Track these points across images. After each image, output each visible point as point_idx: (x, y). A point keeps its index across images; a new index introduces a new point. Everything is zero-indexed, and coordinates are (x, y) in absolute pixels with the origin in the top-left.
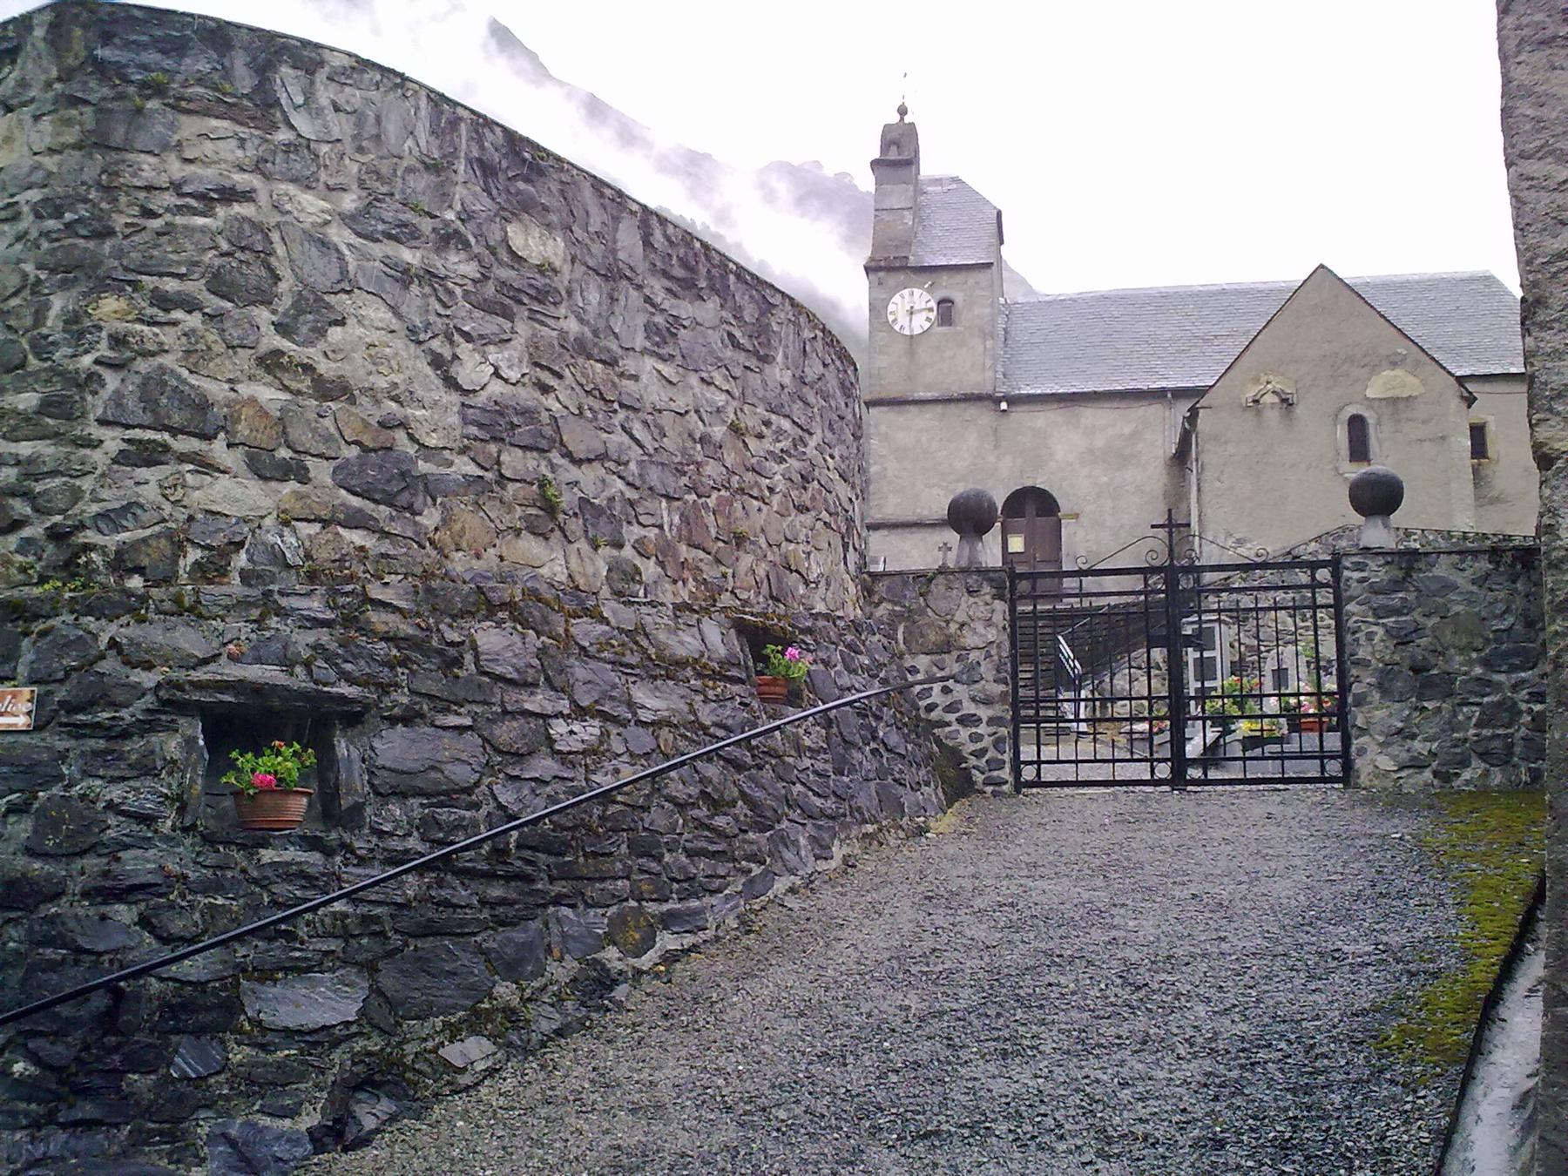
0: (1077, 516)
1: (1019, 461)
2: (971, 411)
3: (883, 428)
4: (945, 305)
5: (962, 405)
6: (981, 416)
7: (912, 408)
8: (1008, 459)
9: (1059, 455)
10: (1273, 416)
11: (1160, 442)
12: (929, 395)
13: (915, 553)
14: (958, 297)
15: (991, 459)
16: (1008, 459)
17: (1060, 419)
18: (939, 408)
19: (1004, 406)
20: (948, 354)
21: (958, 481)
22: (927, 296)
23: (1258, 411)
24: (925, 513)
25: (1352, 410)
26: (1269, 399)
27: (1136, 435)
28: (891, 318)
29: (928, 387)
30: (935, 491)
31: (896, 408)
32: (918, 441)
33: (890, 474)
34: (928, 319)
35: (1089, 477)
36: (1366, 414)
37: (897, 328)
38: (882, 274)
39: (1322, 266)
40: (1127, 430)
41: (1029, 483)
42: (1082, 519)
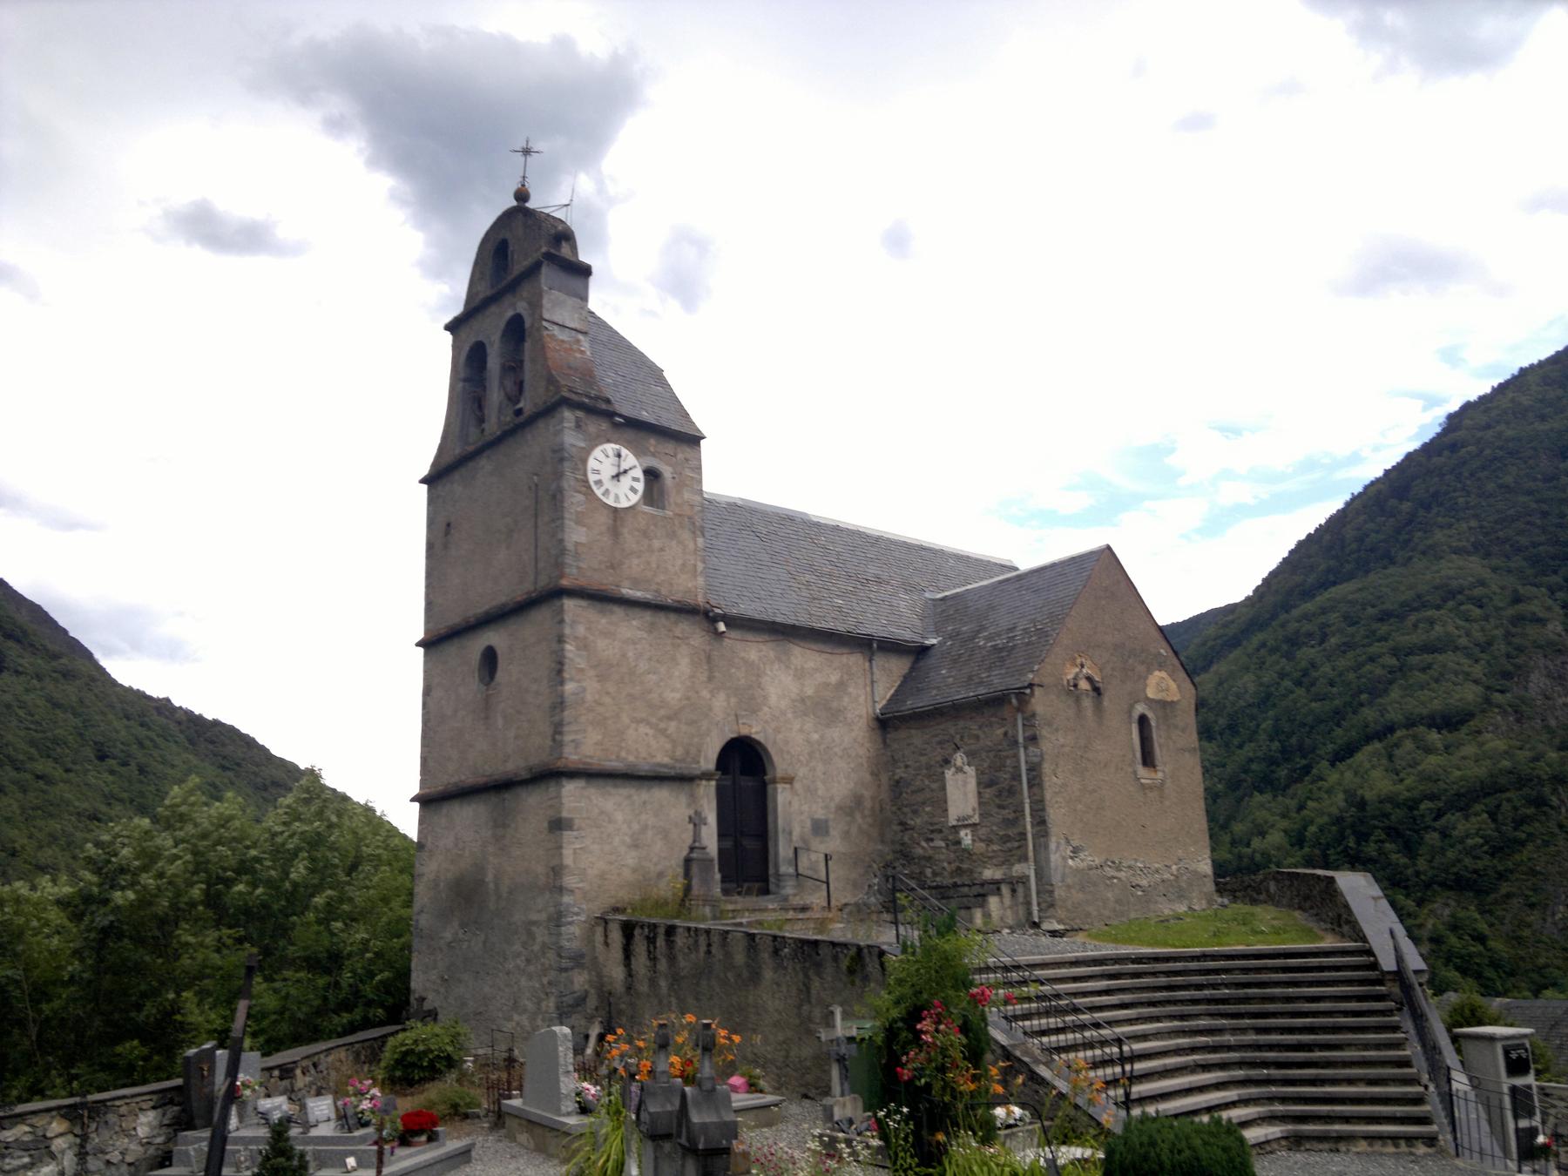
0: (789, 780)
1: (733, 700)
2: (684, 627)
3: (581, 630)
4: (651, 475)
5: (673, 616)
6: (693, 635)
7: (619, 611)
8: (722, 696)
9: (773, 700)
10: (1087, 703)
11: (862, 699)
12: (638, 594)
13: (619, 817)
14: (667, 472)
15: (705, 694)
16: (722, 696)
17: (772, 654)
18: (648, 616)
19: (722, 627)
20: (657, 544)
21: (669, 718)
22: (629, 459)
23: (1078, 700)
24: (631, 759)
25: (1140, 708)
26: (1084, 685)
27: (841, 685)
28: (592, 478)
29: (636, 583)
30: (643, 729)
31: (599, 605)
32: (624, 655)
33: (589, 697)
34: (633, 490)
35: (801, 730)
36: (1150, 715)
37: (599, 492)
38: (580, 414)
39: (1109, 548)
40: (834, 678)
41: (744, 731)
42: (797, 785)
